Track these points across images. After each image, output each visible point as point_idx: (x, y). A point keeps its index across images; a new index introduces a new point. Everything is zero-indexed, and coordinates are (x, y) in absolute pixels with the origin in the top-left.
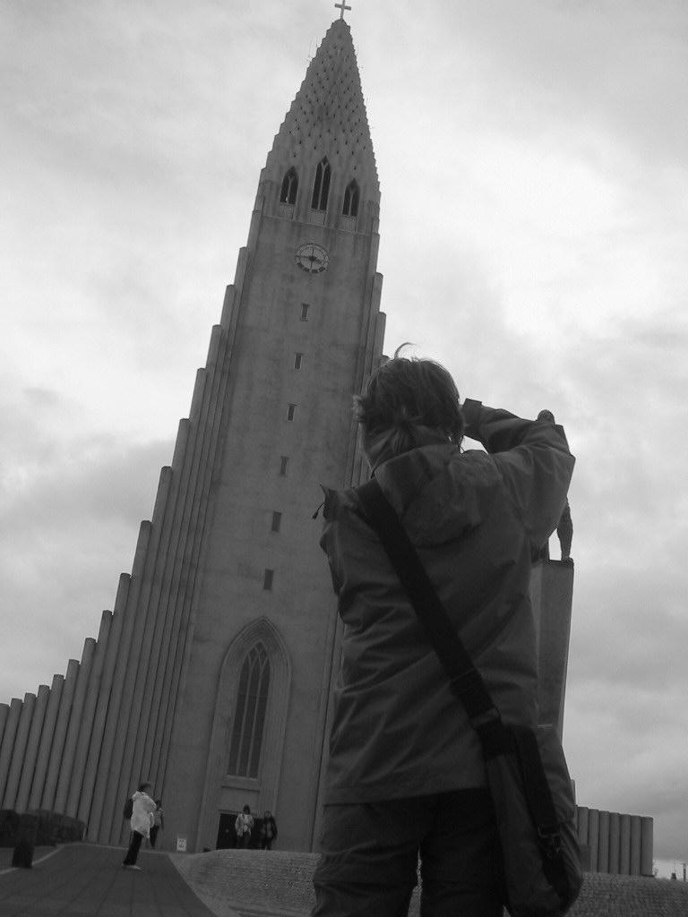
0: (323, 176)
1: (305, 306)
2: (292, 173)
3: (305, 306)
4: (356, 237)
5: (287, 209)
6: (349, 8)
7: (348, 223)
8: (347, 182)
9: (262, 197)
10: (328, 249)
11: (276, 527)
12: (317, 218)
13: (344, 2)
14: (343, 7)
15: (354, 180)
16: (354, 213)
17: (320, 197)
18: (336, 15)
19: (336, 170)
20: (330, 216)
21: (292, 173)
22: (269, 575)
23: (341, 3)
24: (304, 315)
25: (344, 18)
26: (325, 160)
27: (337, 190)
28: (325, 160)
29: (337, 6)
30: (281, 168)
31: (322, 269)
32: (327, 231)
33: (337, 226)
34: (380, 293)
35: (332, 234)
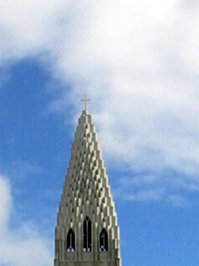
2: (71, 231)
9: (57, 250)
21: (71, 231)
26: (87, 218)
27: (95, 238)
30: (65, 231)
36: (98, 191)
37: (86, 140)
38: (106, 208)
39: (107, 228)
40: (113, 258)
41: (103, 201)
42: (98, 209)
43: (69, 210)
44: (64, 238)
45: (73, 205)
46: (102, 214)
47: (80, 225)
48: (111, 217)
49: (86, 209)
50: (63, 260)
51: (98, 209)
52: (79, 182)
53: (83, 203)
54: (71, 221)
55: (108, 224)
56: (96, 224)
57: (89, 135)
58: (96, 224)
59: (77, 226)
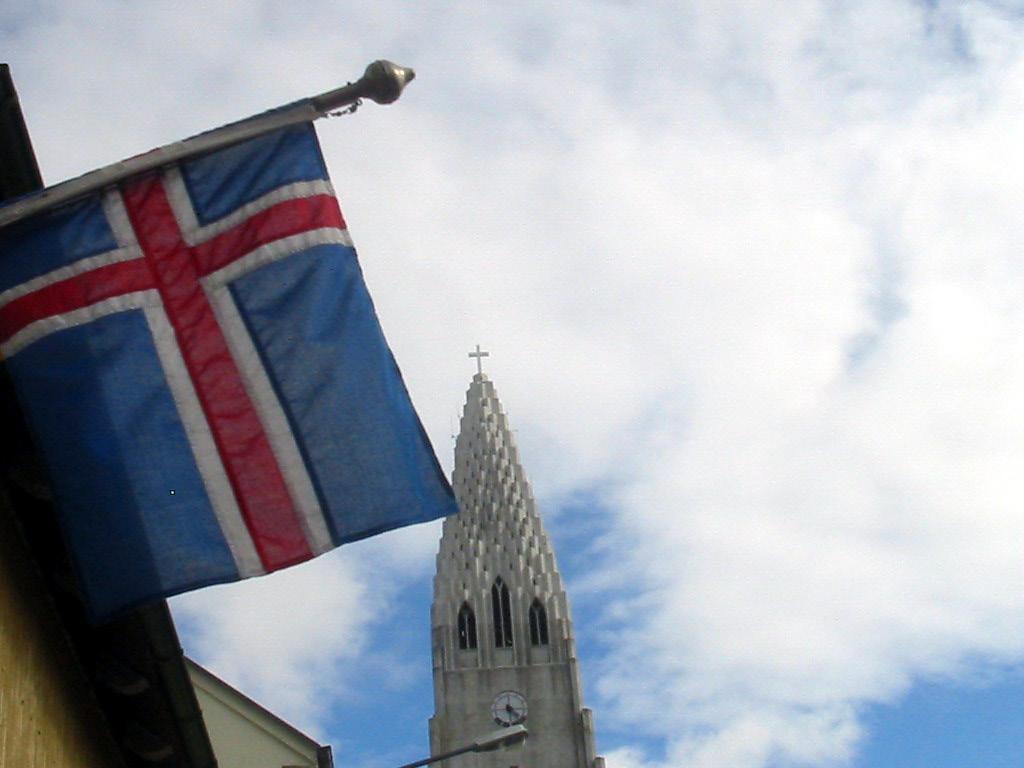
0: (501, 598)
2: (466, 607)
4: (552, 669)
5: (468, 655)
6: (486, 354)
7: (540, 653)
8: (529, 603)
9: (438, 649)
10: (524, 692)
12: (504, 658)
13: (478, 347)
14: (478, 355)
16: (545, 640)
19: (518, 592)
20: (519, 653)
21: (466, 607)
23: (475, 351)
26: (499, 580)
27: (520, 618)
29: (471, 355)
30: (454, 608)
32: (520, 671)
33: (529, 661)
35: (524, 673)
36: (518, 525)
37: (486, 428)
38: (538, 558)
39: (542, 594)
40: (560, 656)
41: (531, 544)
42: (522, 559)
43: (460, 564)
44: (452, 622)
45: (467, 554)
46: (531, 571)
47: (486, 592)
48: (549, 576)
49: (494, 559)
50: (453, 668)
51: (522, 559)
52: (477, 508)
53: (487, 550)
54: (464, 587)
55: (545, 588)
56: (520, 591)
57: (490, 419)
58: (520, 591)
59: (479, 597)
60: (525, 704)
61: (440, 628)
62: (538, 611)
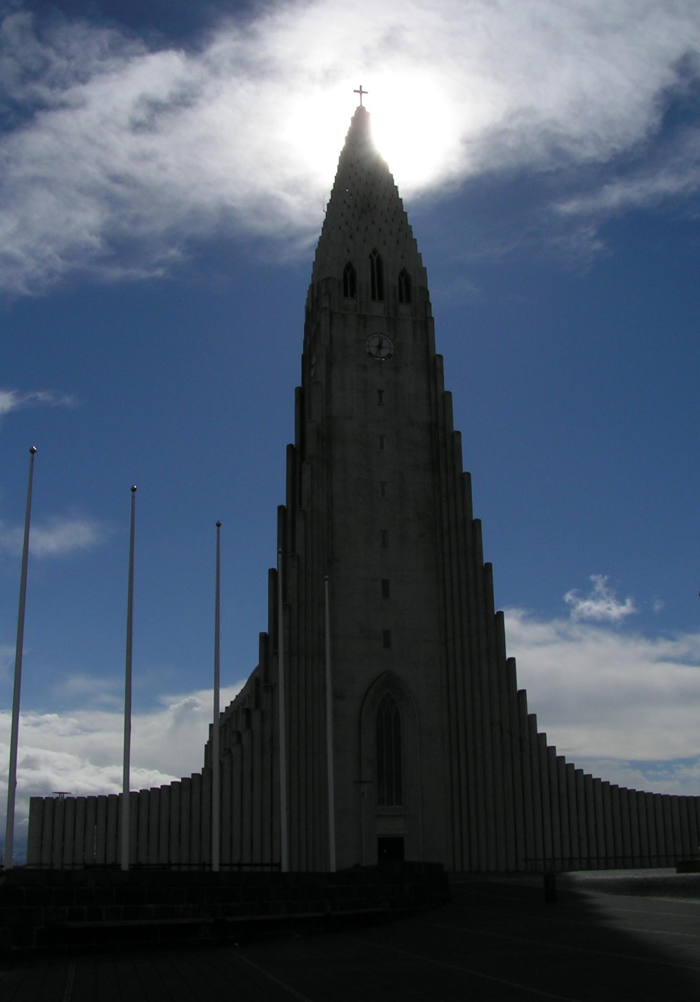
1: (380, 392)
2: (349, 267)
3: (380, 392)
7: (405, 310)
10: (392, 337)
11: (386, 593)
12: (377, 308)
15: (404, 268)
17: (378, 290)
18: (354, 102)
21: (349, 267)
22: (386, 634)
24: (381, 400)
25: (363, 105)
26: (375, 252)
27: (391, 279)
28: (375, 252)
31: (389, 356)
34: (442, 372)
60: (392, 344)
61: (329, 278)
62: (404, 277)
